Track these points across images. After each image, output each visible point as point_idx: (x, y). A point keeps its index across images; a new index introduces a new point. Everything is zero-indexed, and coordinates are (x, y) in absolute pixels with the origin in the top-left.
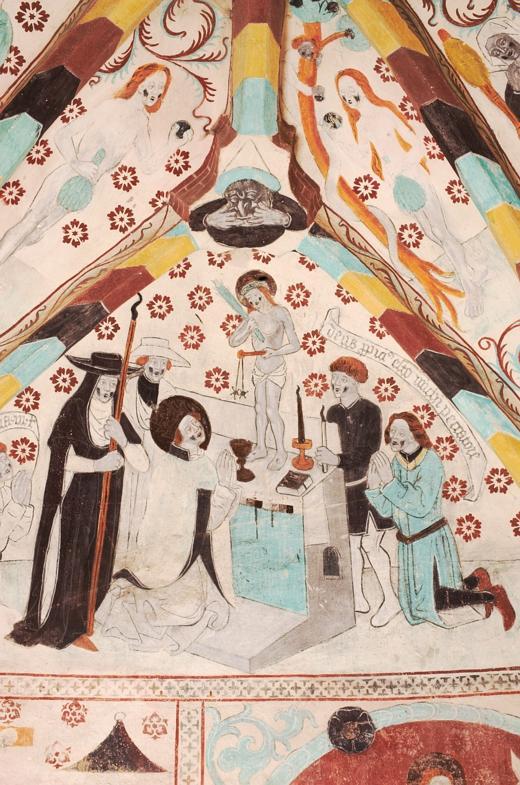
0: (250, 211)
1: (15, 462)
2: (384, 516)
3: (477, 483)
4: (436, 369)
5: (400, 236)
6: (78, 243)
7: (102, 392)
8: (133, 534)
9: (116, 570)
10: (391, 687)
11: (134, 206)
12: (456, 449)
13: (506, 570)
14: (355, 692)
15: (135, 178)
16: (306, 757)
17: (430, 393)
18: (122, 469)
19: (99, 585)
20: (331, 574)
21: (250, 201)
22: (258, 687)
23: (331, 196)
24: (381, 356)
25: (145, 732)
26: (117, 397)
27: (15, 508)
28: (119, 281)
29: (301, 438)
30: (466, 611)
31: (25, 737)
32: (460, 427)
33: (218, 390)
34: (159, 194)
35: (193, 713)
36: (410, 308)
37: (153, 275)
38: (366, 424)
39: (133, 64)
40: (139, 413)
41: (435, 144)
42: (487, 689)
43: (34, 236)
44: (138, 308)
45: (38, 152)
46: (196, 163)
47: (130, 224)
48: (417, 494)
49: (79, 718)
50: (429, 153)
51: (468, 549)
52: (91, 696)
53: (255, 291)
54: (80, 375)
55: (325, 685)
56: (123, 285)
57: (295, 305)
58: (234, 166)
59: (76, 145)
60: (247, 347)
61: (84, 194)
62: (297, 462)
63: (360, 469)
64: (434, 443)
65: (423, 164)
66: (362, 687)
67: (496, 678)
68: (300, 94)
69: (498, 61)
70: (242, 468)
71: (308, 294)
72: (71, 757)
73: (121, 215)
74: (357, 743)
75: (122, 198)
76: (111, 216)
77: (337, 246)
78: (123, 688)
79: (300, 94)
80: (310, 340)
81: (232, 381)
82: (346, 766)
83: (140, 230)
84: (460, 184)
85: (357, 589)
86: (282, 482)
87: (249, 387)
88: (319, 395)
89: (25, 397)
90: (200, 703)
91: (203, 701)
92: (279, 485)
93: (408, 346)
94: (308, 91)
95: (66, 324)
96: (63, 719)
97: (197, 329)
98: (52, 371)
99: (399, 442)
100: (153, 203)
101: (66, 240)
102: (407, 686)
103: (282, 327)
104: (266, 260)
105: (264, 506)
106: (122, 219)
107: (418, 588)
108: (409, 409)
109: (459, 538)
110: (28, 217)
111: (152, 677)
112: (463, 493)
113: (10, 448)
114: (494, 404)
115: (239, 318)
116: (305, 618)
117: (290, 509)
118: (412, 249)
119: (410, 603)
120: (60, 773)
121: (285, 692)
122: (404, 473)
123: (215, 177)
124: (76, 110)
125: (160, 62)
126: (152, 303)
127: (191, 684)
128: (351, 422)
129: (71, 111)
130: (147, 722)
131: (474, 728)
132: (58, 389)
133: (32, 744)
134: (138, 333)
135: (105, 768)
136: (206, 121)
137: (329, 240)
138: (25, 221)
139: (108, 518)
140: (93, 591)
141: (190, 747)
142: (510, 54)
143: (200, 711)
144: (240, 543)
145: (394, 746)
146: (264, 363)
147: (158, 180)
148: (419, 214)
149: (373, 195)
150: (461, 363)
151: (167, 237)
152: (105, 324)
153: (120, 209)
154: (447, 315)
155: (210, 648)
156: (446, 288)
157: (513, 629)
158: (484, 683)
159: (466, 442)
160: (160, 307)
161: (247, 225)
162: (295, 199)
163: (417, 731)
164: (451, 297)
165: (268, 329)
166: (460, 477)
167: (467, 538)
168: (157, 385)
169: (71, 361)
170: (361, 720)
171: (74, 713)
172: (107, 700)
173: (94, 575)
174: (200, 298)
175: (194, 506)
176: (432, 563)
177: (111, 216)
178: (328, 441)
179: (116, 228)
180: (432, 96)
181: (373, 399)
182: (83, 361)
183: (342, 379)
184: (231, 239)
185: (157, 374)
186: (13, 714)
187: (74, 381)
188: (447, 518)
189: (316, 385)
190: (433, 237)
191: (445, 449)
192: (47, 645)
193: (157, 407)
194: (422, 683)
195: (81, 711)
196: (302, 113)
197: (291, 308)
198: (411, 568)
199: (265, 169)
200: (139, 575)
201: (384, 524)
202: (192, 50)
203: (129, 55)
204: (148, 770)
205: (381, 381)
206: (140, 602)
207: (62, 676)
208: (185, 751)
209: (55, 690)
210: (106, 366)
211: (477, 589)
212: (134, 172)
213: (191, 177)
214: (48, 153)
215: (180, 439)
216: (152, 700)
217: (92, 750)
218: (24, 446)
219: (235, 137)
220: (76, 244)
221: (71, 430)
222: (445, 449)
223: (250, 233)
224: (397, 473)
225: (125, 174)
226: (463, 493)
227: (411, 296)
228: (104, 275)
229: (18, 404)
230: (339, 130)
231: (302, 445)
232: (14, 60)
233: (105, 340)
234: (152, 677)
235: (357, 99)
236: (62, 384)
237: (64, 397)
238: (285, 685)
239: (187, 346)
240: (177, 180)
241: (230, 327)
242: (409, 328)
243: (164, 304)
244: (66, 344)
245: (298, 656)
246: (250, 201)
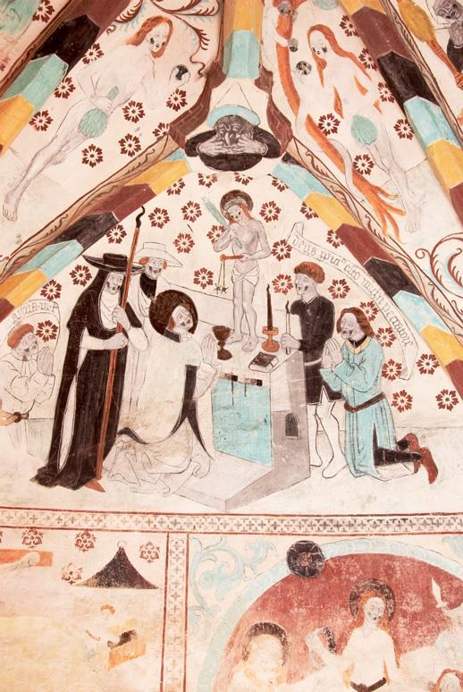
0: (234, 141)
1: (40, 340)
2: (335, 390)
3: (410, 365)
4: (380, 272)
5: (355, 165)
6: (95, 164)
7: (111, 286)
8: (134, 400)
9: (120, 428)
10: (338, 526)
11: (140, 135)
12: (393, 338)
13: (431, 435)
14: (309, 529)
15: (142, 112)
16: (269, 579)
17: (374, 292)
18: (126, 347)
19: (106, 440)
20: (291, 435)
21: (235, 133)
22: (232, 523)
23: (300, 131)
24: (335, 262)
25: (142, 557)
26: (123, 290)
27: (39, 377)
28: (128, 196)
29: (270, 326)
30: (399, 467)
31: (46, 559)
32: (397, 320)
33: (204, 286)
34: (161, 125)
35: (180, 543)
36: (361, 223)
37: (154, 191)
38: (323, 315)
39: (143, 16)
40: (141, 302)
41: (387, 90)
42: (414, 530)
43: (59, 157)
44: (141, 219)
45: (63, 87)
46: (192, 100)
47: (137, 150)
48: (361, 373)
49: (89, 544)
50: (382, 97)
51: (401, 417)
52: (99, 527)
53: (235, 207)
54: (94, 271)
55: (285, 523)
56: (130, 199)
57: (268, 219)
59: (95, 83)
60: (228, 252)
61: (100, 124)
62: (266, 346)
63: (317, 352)
64: (376, 331)
65: (376, 105)
66: (315, 525)
67: (422, 521)
68: (278, 45)
69: (442, 20)
70: (222, 349)
71: (278, 211)
72: (82, 575)
73: (130, 142)
74: (309, 570)
75: (130, 128)
76: (122, 142)
77: (303, 172)
78: (125, 522)
79: (278, 45)
80: (279, 248)
81: (215, 279)
82: (301, 587)
83: (144, 155)
84: (407, 122)
85: (312, 448)
86: (254, 361)
87: (229, 284)
88: (285, 292)
89: (49, 288)
90: (185, 535)
91: (188, 533)
92: (251, 363)
93: (358, 253)
94: (284, 43)
95: (82, 228)
96: (77, 545)
97: (188, 236)
98: (72, 267)
99: (348, 331)
100: (156, 132)
101: (85, 161)
102: (351, 525)
103: (256, 237)
104: (245, 182)
105: (239, 380)
106: (130, 146)
107: (360, 447)
108: (357, 305)
109: (394, 409)
110: (55, 141)
111: (148, 513)
112: (399, 373)
113: (36, 328)
114: (426, 302)
115: (222, 229)
116: (270, 470)
117: (259, 383)
118: (364, 175)
119: (354, 460)
120: (73, 588)
121: (253, 528)
122: (351, 356)
123: (207, 113)
124: (95, 53)
126: (153, 215)
127: (179, 520)
128: (310, 314)
129: (91, 54)
130: (144, 549)
131: (403, 560)
132: (76, 282)
133: (51, 565)
134: (140, 238)
135: (109, 585)
136: (200, 66)
137: (298, 167)
138: (52, 144)
139: (114, 386)
140: (102, 444)
141: (177, 570)
142: (453, 14)
143: (185, 542)
144: (219, 409)
145: (339, 573)
146: (242, 266)
148: (372, 147)
149: (335, 130)
150: (401, 269)
151: (166, 161)
152: (115, 231)
153: (129, 137)
154: (390, 230)
155: (194, 491)
156: (391, 208)
157: (435, 483)
158: (412, 524)
159: (402, 333)
160: (159, 218)
161: (231, 153)
162: (272, 133)
163: (358, 561)
164: (394, 215)
165: (246, 238)
166: (397, 361)
167: (401, 409)
168: (155, 281)
169: (87, 260)
170: (312, 552)
171: (85, 541)
172: (112, 531)
173: (102, 431)
174: (191, 212)
175: (183, 378)
176: (372, 428)
177: (122, 142)
178: (291, 329)
180: (388, 48)
181: (328, 296)
183: (304, 280)
184: (219, 163)
185: (155, 272)
186: (37, 541)
187: (89, 276)
188: (385, 393)
189: (283, 284)
190: (380, 164)
191: (385, 338)
192: (64, 486)
193: (155, 299)
194: (362, 524)
195: (91, 539)
196: (279, 62)
197: (264, 222)
198: (355, 432)
199: (249, 107)
200: (139, 432)
201: (334, 396)
202: (191, 6)
203: (139, 8)
204: (143, 587)
205: (335, 282)
206: (139, 454)
207: (75, 511)
208: (174, 573)
209: (70, 522)
210: (115, 265)
211: (407, 451)
212: (141, 107)
213: (187, 112)
214: (72, 88)
215: (173, 324)
216: (147, 532)
217: (99, 570)
218: (48, 328)
219: (224, 79)
221: (85, 315)
222: (385, 338)
223: (233, 160)
224: (346, 356)
225: (133, 108)
226: (399, 373)
227: (362, 213)
228: (115, 191)
229: (43, 293)
230: (309, 75)
231: (271, 332)
232: (45, 9)
233: (114, 244)
234: (148, 513)
235: (325, 50)
237: (81, 289)
238: (253, 522)
239: (180, 250)
240: (175, 115)
241: (214, 236)
242: (356, 239)
243: (162, 216)
245: (266, 498)
246: (235, 133)
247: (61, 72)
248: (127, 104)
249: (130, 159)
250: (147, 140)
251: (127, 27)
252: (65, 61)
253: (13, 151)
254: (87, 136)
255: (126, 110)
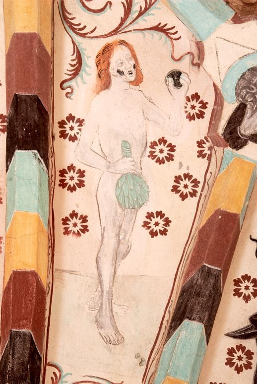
11: (188, 168)
15: (170, 145)
34: (200, 144)
39: (88, 57)
43: (123, 248)
46: (209, 97)
56: (212, 237)
58: (224, 71)
61: (139, 187)
73: (182, 183)
75: (171, 170)
76: (175, 189)
100: (201, 154)
101: (153, 234)
106: (186, 186)
124: (75, 125)
125: (110, 40)
129: (72, 128)
132: (239, 370)
136: (188, 59)
147: (188, 135)
151: (222, 171)
153: (178, 179)
169: (235, 337)
177: (175, 189)
179: (186, 196)
182: (245, 331)
187: (249, 354)
212: (165, 142)
213: (213, 110)
214: (82, 173)
220: (164, 232)
225: (158, 148)
236: (240, 363)
240: (204, 123)
244: (201, 320)
247: (35, 162)
248: (149, 149)
249: (196, 199)
250: (198, 168)
251: (82, 78)
252: (30, 149)
253: (71, 272)
254: (135, 208)
255: (152, 155)
